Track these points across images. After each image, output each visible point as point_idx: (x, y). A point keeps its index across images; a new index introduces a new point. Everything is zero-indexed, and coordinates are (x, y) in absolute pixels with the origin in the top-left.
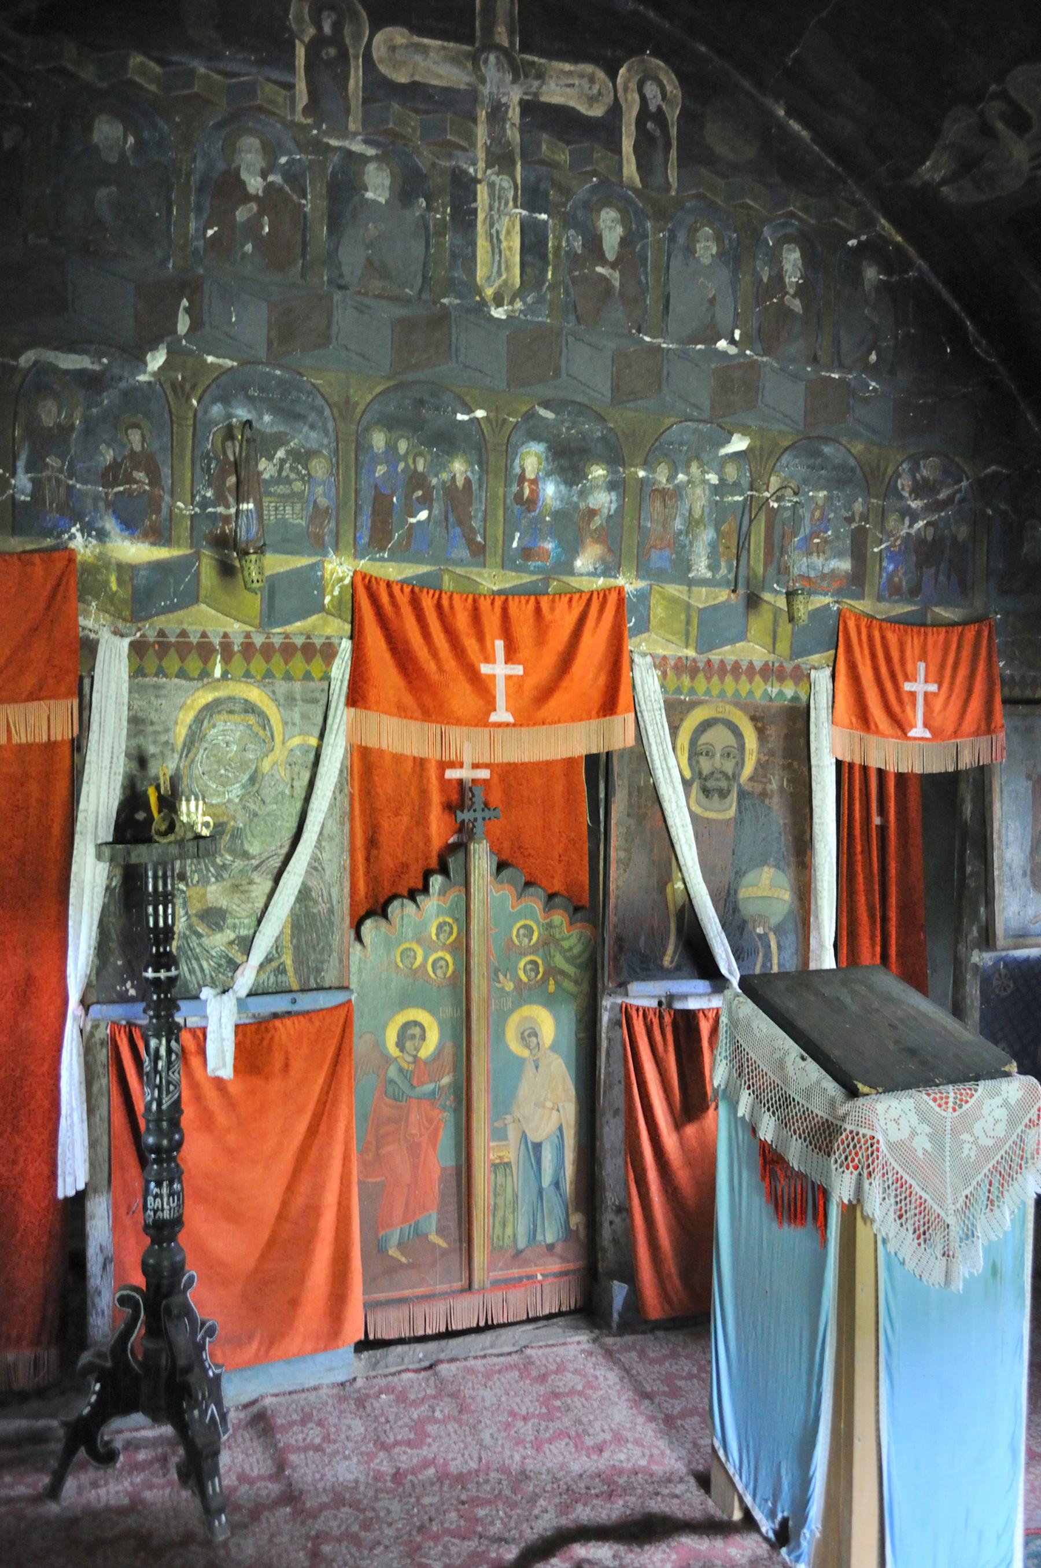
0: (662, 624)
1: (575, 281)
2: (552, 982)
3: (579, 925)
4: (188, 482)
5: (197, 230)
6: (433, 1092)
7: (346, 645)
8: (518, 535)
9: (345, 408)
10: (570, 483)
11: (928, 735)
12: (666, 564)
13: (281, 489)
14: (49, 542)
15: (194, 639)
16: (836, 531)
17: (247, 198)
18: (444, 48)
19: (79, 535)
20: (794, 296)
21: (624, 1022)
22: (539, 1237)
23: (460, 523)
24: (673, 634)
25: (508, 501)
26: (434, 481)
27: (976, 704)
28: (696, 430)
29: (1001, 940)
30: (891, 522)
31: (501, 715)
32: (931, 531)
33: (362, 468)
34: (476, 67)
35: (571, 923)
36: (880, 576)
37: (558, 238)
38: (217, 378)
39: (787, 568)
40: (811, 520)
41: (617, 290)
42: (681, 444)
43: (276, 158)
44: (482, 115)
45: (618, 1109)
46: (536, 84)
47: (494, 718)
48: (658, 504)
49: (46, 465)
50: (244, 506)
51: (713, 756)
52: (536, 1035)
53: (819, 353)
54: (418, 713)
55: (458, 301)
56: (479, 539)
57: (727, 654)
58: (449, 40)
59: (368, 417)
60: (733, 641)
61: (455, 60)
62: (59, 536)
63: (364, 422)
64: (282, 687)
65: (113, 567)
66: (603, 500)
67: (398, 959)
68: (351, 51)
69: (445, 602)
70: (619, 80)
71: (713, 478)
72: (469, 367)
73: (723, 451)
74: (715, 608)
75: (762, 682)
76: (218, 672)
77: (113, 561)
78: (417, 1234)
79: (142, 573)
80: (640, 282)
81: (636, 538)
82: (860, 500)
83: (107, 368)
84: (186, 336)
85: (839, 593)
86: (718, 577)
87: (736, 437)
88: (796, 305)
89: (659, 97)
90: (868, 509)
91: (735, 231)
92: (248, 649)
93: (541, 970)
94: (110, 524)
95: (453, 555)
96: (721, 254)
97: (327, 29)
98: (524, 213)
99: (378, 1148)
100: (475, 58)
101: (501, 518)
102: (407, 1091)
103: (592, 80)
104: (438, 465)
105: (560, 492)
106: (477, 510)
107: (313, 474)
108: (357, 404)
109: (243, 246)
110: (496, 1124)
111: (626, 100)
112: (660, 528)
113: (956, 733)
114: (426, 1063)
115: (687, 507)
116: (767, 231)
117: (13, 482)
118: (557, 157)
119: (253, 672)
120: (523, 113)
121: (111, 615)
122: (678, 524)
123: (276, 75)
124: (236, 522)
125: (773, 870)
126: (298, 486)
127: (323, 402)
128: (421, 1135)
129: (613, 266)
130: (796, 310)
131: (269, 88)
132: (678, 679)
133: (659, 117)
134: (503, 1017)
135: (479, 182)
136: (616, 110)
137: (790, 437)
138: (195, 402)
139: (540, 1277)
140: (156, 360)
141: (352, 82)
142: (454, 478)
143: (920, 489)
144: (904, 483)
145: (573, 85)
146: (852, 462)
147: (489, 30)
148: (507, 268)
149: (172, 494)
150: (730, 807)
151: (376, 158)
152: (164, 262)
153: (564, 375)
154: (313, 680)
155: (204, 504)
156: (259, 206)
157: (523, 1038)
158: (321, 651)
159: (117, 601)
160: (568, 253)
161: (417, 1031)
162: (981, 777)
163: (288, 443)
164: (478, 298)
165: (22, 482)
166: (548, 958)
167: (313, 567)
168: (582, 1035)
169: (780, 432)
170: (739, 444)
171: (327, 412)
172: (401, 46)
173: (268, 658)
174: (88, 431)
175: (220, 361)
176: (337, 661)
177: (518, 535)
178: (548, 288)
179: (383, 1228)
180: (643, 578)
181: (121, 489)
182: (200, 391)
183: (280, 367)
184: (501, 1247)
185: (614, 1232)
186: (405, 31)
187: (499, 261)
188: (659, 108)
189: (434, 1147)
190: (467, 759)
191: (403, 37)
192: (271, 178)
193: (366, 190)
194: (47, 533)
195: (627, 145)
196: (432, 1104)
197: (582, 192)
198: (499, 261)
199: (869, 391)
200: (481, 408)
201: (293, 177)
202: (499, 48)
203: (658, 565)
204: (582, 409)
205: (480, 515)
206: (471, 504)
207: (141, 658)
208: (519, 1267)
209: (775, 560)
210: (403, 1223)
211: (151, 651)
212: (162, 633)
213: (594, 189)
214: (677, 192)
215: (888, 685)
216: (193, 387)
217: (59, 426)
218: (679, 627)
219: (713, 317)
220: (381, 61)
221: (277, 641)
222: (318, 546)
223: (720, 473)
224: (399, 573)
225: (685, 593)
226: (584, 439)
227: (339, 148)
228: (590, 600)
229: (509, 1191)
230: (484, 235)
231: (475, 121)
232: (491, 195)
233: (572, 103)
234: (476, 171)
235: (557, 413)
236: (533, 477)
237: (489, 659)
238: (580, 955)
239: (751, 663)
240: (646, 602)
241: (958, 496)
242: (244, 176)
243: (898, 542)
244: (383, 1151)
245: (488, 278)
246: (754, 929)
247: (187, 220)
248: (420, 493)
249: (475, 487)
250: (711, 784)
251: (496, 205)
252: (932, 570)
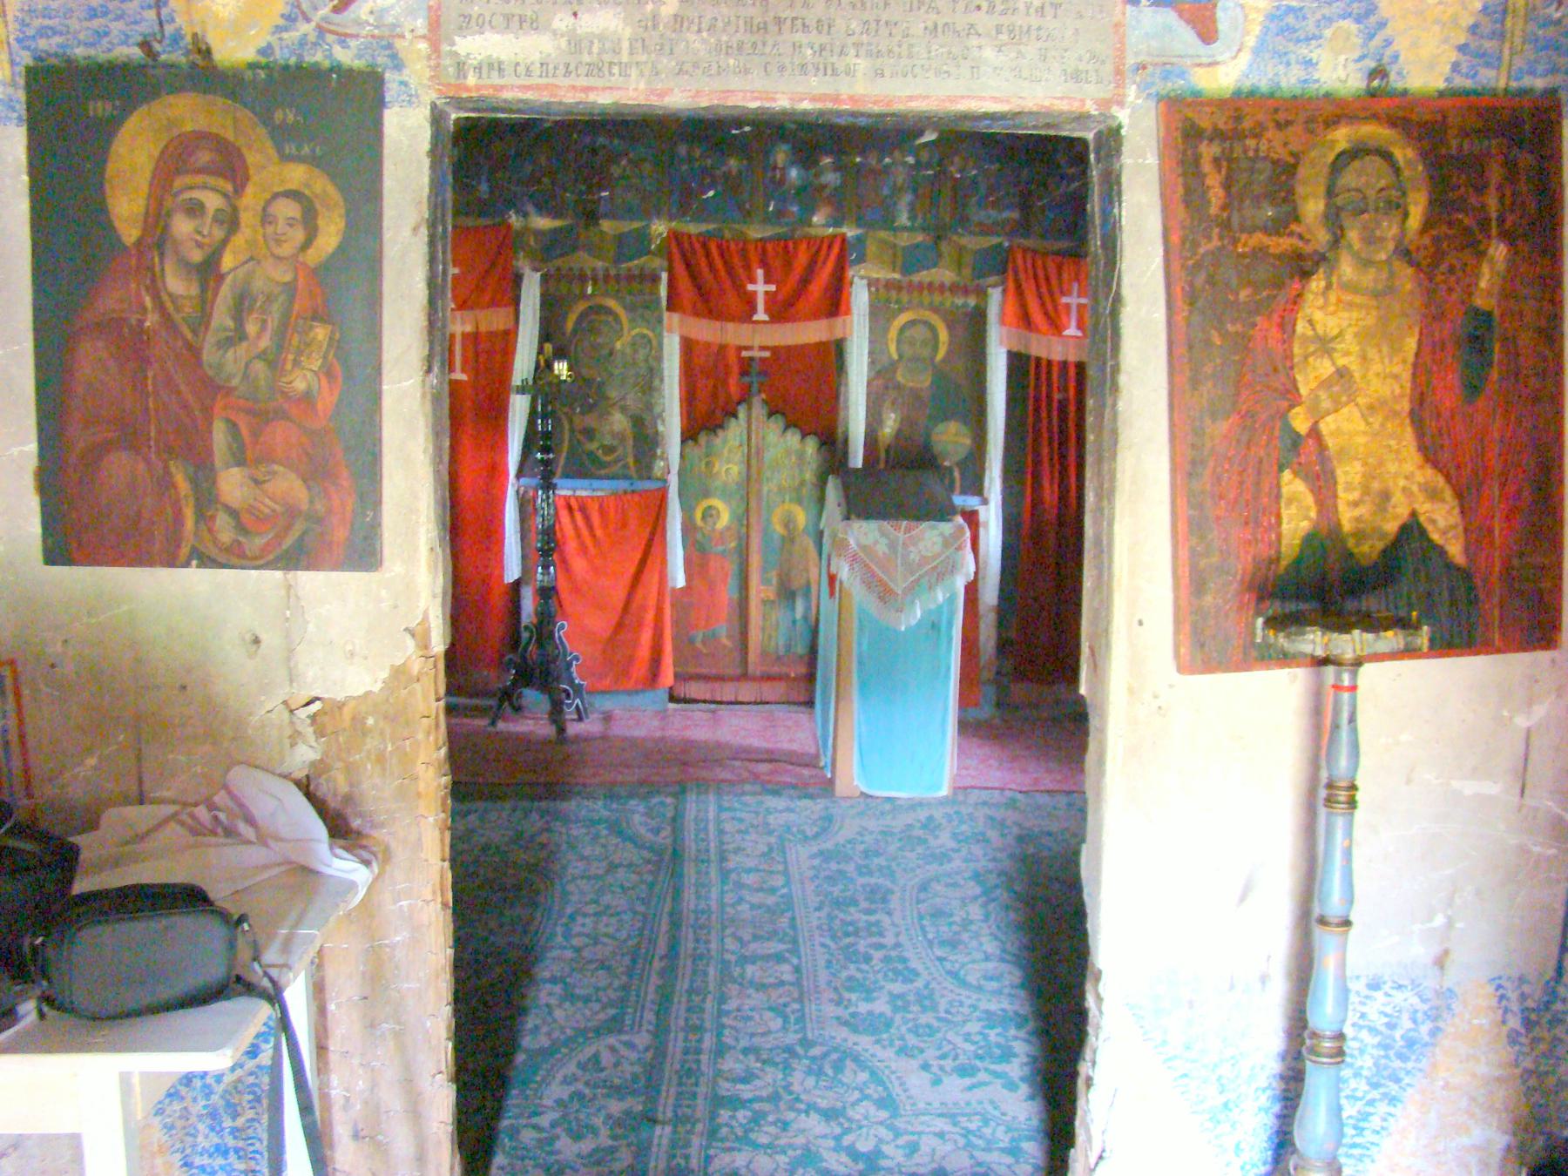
7: (664, 276)
10: (807, 168)
11: (1079, 334)
14: (498, 220)
31: (761, 315)
64: (629, 299)
66: (831, 178)
71: (911, 160)
85: (1012, 234)
92: (607, 277)
94: (530, 208)
155: (581, 193)
215: (1047, 299)
222: (648, 214)
223: (916, 156)
237: (753, 281)
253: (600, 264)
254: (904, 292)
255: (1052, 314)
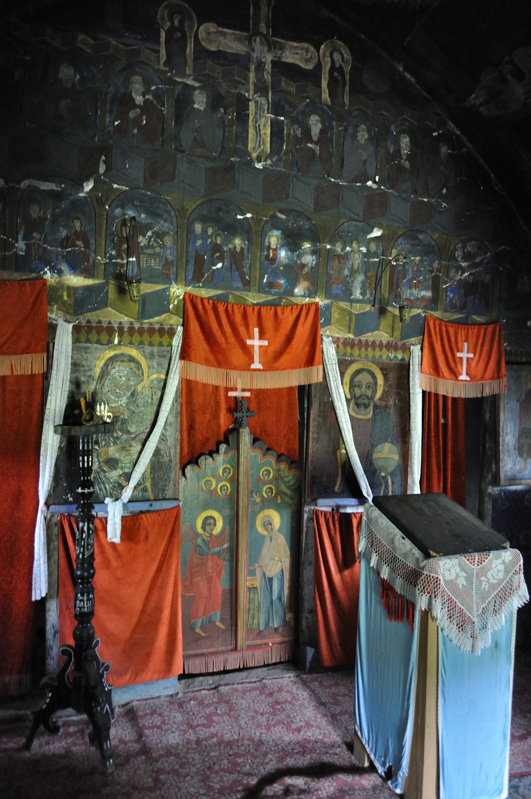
0: (337, 321)
1: (297, 150)
2: (279, 498)
3: (293, 470)
4: (103, 247)
5: (110, 121)
6: (219, 552)
7: (180, 329)
8: (266, 276)
9: (181, 212)
10: (293, 251)
11: (468, 379)
12: (340, 292)
13: (149, 251)
14: (34, 275)
15: (105, 325)
16: (424, 277)
17: (135, 106)
18: (234, 34)
19: (48, 272)
20: (406, 160)
21: (315, 518)
22: (271, 625)
23: (238, 269)
24: (343, 326)
25: (262, 259)
26: (225, 249)
27: (492, 364)
28: (356, 226)
29: (502, 482)
30: (452, 273)
31: (257, 365)
32: (471, 277)
33: (190, 241)
34: (250, 44)
35: (290, 469)
36: (446, 300)
37: (289, 129)
38: (119, 195)
39: (400, 295)
40: (412, 271)
41: (318, 155)
42: (348, 232)
43: (150, 87)
44: (253, 67)
45: (311, 562)
46: (280, 52)
47: (253, 366)
48: (336, 262)
49: (33, 237)
50: (131, 259)
51: (361, 387)
52: (271, 524)
53: (418, 188)
54: (215, 363)
55: (238, 160)
56: (247, 278)
57: (369, 337)
58: (237, 30)
59: (193, 216)
60: (372, 331)
61: (240, 40)
62: (39, 272)
63: (191, 219)
64: (148, 349)
65: (65, 288)
66: (309, 259)
67: (203, 485)
68: (188, 34)
69: (230, 309)
70: (321, 51)
71: (364, 249)
72: (244, 192)
73: (369, 236)
74: (364, 314)
75: (386, 351)
76: (116, 341)
77: (65, 285)
78: (210, 622)
79: (80, 291)
80: (329, 152)
81: (325, 278)
82: (437, 261)
83: (64, 189)
84: (103, 174)
85: (426, 308)
86: (365, 298)
87: (375, 229)
88: (407, 164)
89: (341, 60)
90: (441, 266)
91: (377, 127)
92: (131, 330)
93: (274, 492)
94: (64, 267)
95: (234, 286)
96: (370, 139)
97: (176, 23)
98: (272, 116)
99: (191, 579)
100: (249, 39)
101: (258, 267)
102: (206, 551)
103: (307, 51)
104: (228, 240)
105: (288, 255)
106: (246, 263)
107: (165, 244)
108: (188, 209)
109: (133, 130)
110: (250, 568)
111: (324, 61)
112: (337, 274)
113: (482, 378)
114: (216, 537)
115: (351, 263)
116: (393, 127)
117: (16, 245)
118: (289, 89)
119: (134, 342)
120: (273, 67)
121: (64, 312)
122: (346, 272)
123: (150, 46)
124: (127, 267)
125: (390, 444)
126: (158, 250)
127: (171, 208)
128: (213, 573)
129: (316, 143)
130: (407, 167)
131: (147, 52)
132: (345, 349)
133: (341, 70)
134: (255, 515)
135: (251, 100)
136: (319, 66)
137: (403, 230)
138: (107, 207)
139: (270, 644)
140: (89, 186)
141: (188, 50)
142: (235, 247)
143: (466, 257)
144: (459, 254)
145: (298, 53)
146: (433, 243)
147: (256, 25)
148: (264, 144)
149: (95, 252)
150: (369, 413)
151: (199, 88)
152: (94, 136)
153: (291, 197)
154: (163, 346)
155: (111, 257)
156: (141, 110)
157: (264, 526)
158: (168, 332)
159: (67, 305)
160: (294, 137)
161: (212, 521)
162: (494, 400)
163: (153, 228)
164: (249, 158)
165: (21, 245)
166: (277, 486)
167: (164, 290)
168: (294, 525)
169: (398, 227)
170: (377, 233)
171: (173, 213)
172: (213, 32)
173: (141, 335)
174: (54, 220)
175: (120, 187)
176: (176, 337)
177: (266, 276)
178: (284, 154)
179: (193, 619)
180: (328, 298)
181: (70, 249)
182: (110, 202)
183: (150, 190)
184: (252, 629)
185: (308, 623)
186: (215, 25)
187: (260, 140)
188: (341, 65)
189: (220, 579)
190: (239, 387)
191: (214, 28)
192: (147, 97)
193: (194, 104)
194: (33, 271)
195: (324, 84)
196: (219, 558)
197: (301, 106)
198: (260, 140)
199: (442, 208)
200: (249, 213)
201: (158, 96)
202: (261, 34)
203: (336, 292)
204: (300, 214)
205: (248, 266)
206: (243, 261)
207: (78, 334)
208: (261, 639)
209: (394, 291)
210: (203, 616)
211: (83, 330)
212: (89, 321)
213: (308, 105)
214: (349, 107)
215: (449, 354)
216: (107, 200)
217: (40, 218)
218: (346, 323)
219: (365, 170)
220: (203, 40)
221: (146, 326)
222: (167, 280)
224: (207, 294)
225: (349, 306)
226: (300, 229)
227: (181, 83)
228: (301, 309)
229: (256, 601)
230: (252, 127)
231: (249, 70)
232: (256, 107)
233: (297, 62)
234: (249, 95)
235: (287, 216)
236: (274, 247)
237: (251, 337)
238: (293, 485)
239: (381, 342)
240: (330, 311)
241: (485, 261)
242: (134, 95)
243: (455, 283)
244: (194, 580)
245: (254, 148)
246: (380, 474)
247: (105, 117)
248: (218, 254)
249: (245, 252)
250: (360, 401)
251: (259, 112)
252: (472, 297)
253: (125, 320)
254: (356, 348)
255: (453, 365)
